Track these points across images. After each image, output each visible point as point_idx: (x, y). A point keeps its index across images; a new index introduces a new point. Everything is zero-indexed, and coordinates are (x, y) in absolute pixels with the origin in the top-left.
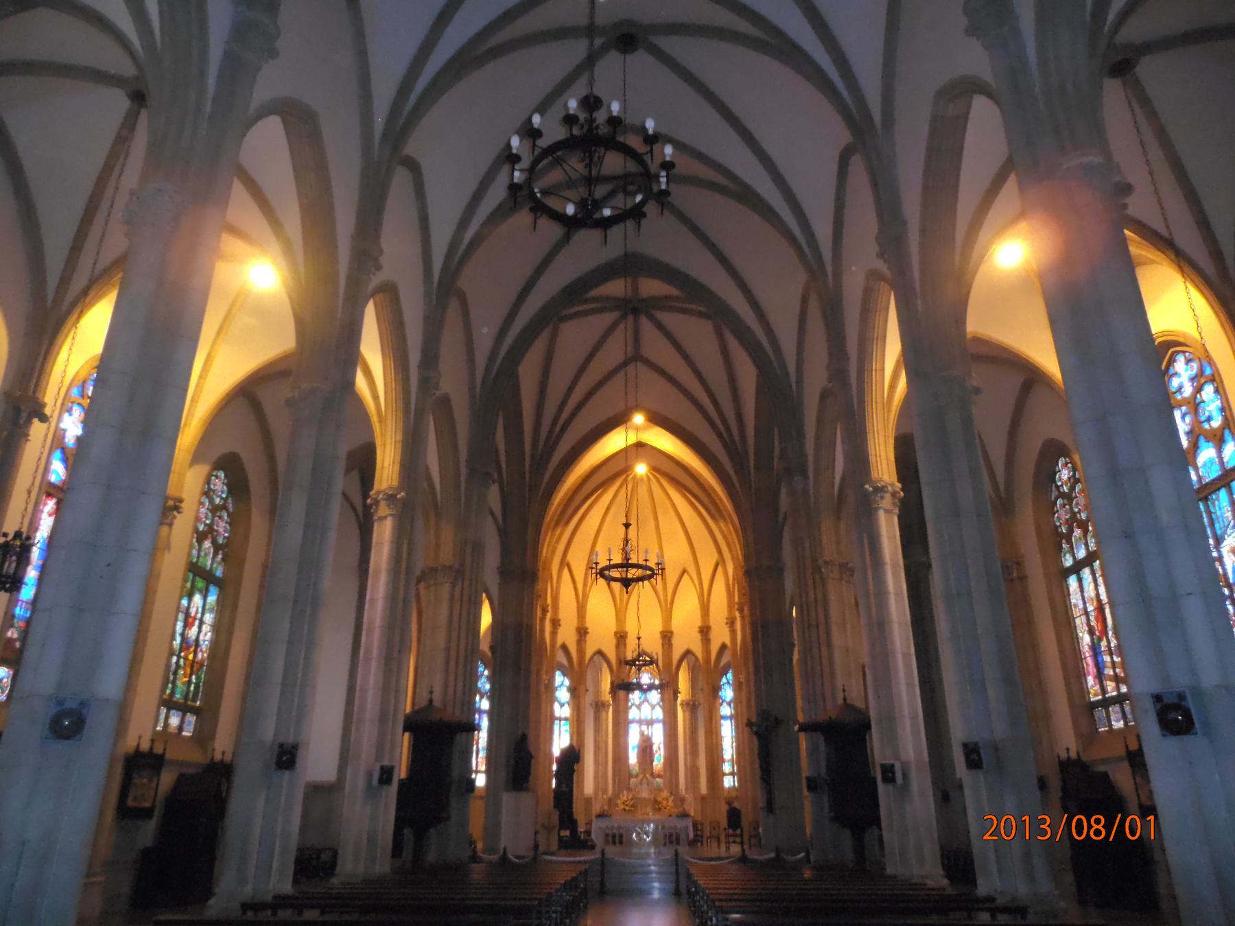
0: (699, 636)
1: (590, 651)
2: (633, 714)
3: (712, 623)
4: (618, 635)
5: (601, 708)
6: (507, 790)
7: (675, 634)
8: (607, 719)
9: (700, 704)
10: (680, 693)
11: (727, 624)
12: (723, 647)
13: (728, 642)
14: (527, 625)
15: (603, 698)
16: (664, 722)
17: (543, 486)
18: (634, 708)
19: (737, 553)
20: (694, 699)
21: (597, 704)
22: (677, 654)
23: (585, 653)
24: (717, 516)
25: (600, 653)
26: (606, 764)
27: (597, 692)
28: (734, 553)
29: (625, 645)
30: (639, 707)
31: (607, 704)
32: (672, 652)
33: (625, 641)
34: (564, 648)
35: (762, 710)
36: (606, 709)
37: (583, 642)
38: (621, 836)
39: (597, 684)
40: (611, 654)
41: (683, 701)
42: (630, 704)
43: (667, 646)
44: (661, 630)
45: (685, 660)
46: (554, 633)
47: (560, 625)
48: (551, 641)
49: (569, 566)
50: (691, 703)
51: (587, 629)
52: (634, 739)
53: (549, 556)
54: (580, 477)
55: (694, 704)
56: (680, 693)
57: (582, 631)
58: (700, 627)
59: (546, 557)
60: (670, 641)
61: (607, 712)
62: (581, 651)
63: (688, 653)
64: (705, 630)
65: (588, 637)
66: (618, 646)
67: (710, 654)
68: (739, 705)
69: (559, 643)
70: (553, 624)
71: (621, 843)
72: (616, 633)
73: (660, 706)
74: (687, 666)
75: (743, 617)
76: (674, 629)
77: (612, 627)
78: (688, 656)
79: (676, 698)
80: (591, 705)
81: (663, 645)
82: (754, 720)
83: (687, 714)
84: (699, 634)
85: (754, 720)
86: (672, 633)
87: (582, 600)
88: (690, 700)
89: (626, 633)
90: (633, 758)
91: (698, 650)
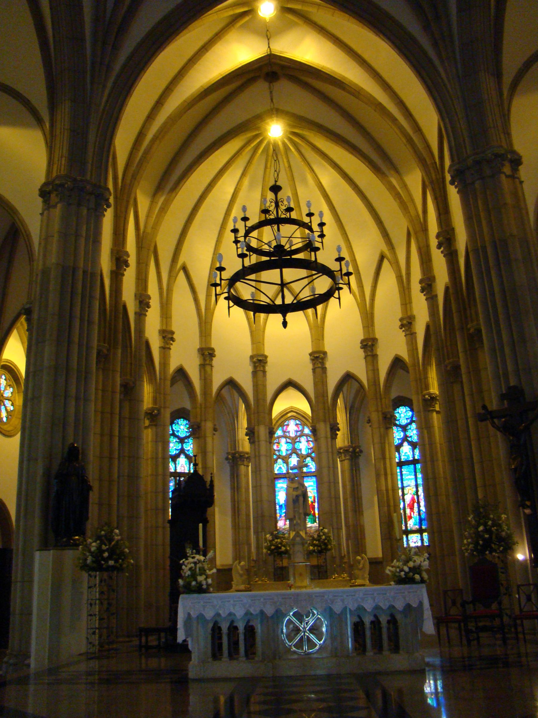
0: (361, 353)
1: (217, 380)
2: (280, 467)
3: (379, 333)
4: (255, 360)
5: (240, 463)
6: (45, 546)
7: (328, 354)
8: (247, 475)
9: (361, 451)
10: (339, 430)
11: (402, 326)
12: (397, 362)
13: (405, 355)
14: (85, 272)
15: (241, 449)
16: (318, 475)
17: (117, 67)
18: (280, 461)
19: (417, 212)
20: (354, 445)
21: (234, 457)
22: (333, 380)
23: (211, 381)
24: (384, 168)
25: (231, 383)
26: (248, 528)
27: (234, 442)
28: (413, 212)
29: (264, 372)
30: (285, 459)
31: (246, 456)
32: (326, 377)
33: (264, 367)
34: (181, 372)
35: (509, 388)
36: (245, 463)
37: (208, 368)
38: (250, 630)
39: (233, 431)
40: (247, 384)
41: (340, 448)
42: (275, 457)
43: (318, 371)
44: (310, 351)
45: (341, 396)
46: (165, 349)
47: (173, 339)
48: (160, 358)
49: (184, 269)
50: (351, 449)
51: (213, 350)
52: (281, 497)
53: (149, 230)
54: (185, 101)
55: (354, 451)
56: (339, 430)
57: (207, 353)
58: (362, 342)
59: (144, 232)
60: (323, 363)
61: (248, 466)
62: (206, 380)
63: (348, 377)
64: (370, 343)
65: (215, 361)
66: (255, 373)
67: (378, 374)
68: (425, 432)
69: (173, 367)
70: (164, 338)
71: (250, 652)
72: (252, 357)
73: (312, 459)
74: (343, 405)
75: (431, 298)
76: (327, 349)
77: (248, 351)
78: (345, 389)
79: (334, 436)
80: (227, 459)
81: (314, 370)
82: (494, 404)
83: (347, 463)
84: (362, 351)
85: (494, 404)
86: (325, 353)
87: (206, 314)
88: (349, 447)
89: (266, 357)
90: (282, 524)
91: (361, 373)
